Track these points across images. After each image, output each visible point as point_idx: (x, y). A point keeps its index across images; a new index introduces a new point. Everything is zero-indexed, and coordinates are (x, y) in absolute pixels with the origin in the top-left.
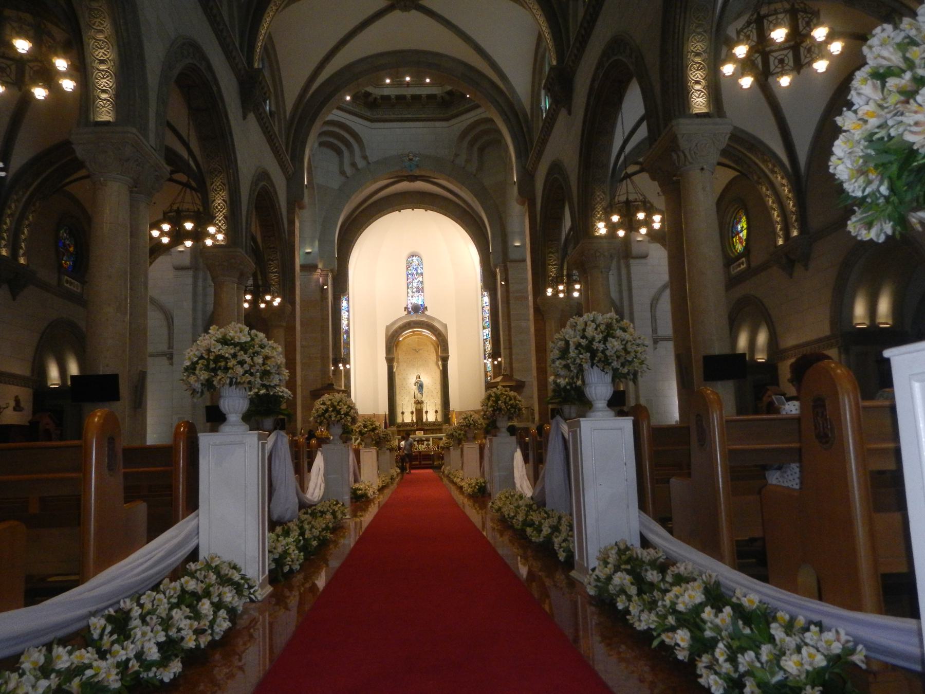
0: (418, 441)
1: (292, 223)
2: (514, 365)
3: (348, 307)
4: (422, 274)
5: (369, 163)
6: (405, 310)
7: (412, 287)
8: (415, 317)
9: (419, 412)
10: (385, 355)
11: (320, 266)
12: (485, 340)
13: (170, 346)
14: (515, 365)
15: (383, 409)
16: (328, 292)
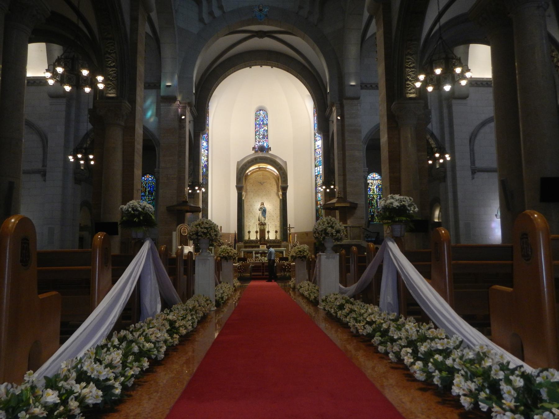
0: (261, 254)
1: (134, 20)
2: (347, 189)
3: (208, 147)
4: (267, 124)
5: (224, 12)
6: (253, 150)
7: (259, 135)
8: (260, 154)
9: (262, 232)
10: (236, 185)
11: (179, 98)
12: (316, 176)
13: (44, 165)
14: (349, 189)
15: (233, 229)
16: (185, 122)
